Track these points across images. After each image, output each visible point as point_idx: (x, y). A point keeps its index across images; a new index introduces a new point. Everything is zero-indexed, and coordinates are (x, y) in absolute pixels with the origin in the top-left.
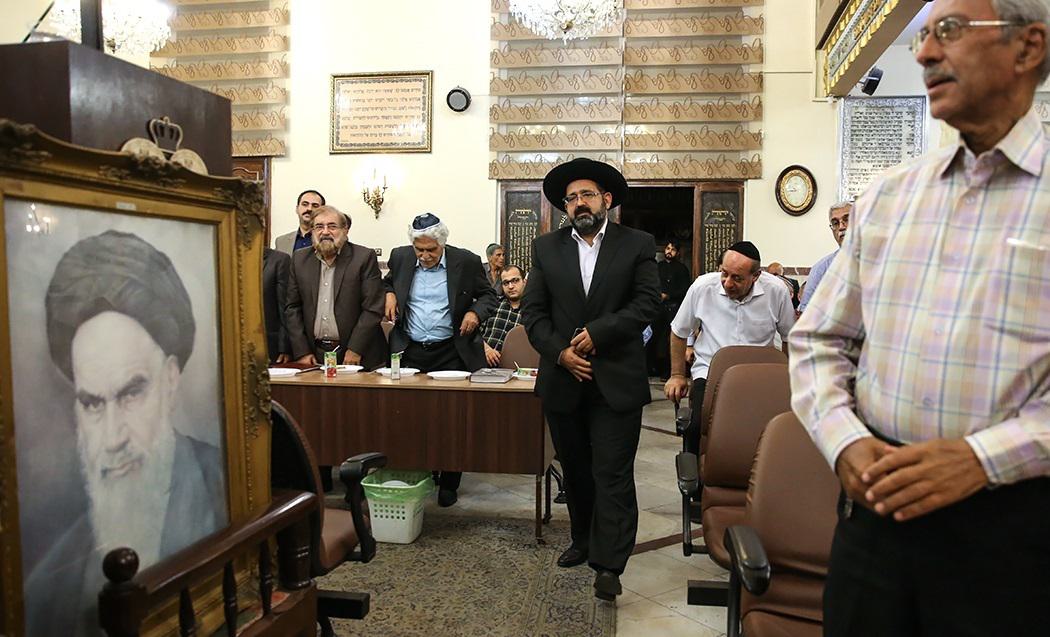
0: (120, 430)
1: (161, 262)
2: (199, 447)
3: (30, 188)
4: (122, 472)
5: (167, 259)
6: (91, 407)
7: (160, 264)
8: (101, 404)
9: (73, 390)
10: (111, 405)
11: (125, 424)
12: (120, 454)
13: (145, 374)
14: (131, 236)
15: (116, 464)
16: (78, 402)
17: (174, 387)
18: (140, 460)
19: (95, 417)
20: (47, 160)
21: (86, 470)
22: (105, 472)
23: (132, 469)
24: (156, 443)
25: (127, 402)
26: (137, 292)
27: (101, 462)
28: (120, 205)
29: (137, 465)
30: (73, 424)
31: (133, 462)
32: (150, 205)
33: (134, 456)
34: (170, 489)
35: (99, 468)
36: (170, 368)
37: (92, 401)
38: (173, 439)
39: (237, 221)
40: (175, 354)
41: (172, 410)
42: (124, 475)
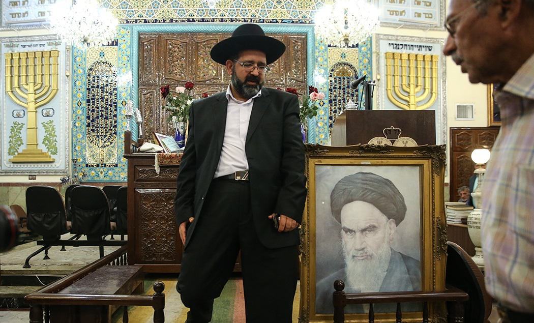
1: (388, 183)
2: (405, 258)
3: (324, 161)
4: (362, 258)
5: (390, 182)
6: (349, 233)
7: (386, 184)
9: (341, 226)
10: (358, 234)
12: (361, 252)
13: (375, 224)
15: (359, 255)
16: (342, 230)
18: (371, 256)
19: (349, 237)
20: (327, 152)
22: (354, 257)
24: (380, 251)
25: (366, 234)
26: (373, 194)
29: (369, 257)
30: (340, 237)
32: (379, 161)
33: (368, 254)
34: (387, 271)
35: (351, 254)
36: (390, 223)
37: (348, 231)
38: (391, 252)
39: (432, 163)
42: (362, 260)
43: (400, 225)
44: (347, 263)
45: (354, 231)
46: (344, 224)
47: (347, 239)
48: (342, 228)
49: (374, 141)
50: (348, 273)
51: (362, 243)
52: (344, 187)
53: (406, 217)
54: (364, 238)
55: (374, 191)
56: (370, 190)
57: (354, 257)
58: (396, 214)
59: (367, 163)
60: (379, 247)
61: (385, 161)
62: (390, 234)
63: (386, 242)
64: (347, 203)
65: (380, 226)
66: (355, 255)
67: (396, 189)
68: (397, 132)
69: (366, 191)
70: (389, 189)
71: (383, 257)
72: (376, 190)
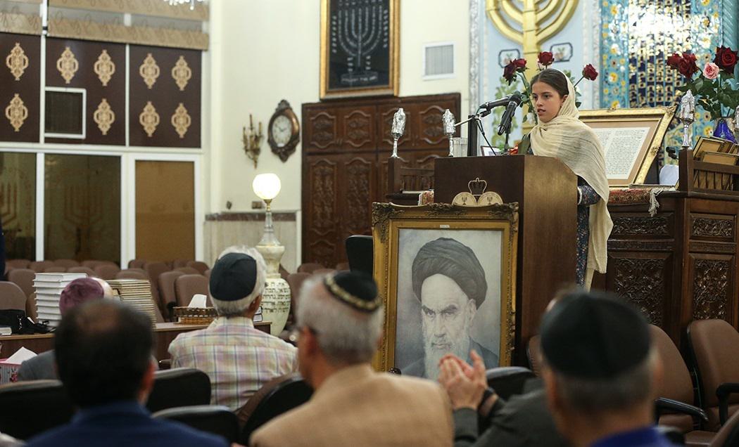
0: (441, 328)
1: (468, 252)
6: (429, 314)
7: (468, 254)
8: (433, 314)
10: (438, 316)
11: (444, 326)
12: (441, 339)
13: (456, 305)
14: (451, 239)
15: (437, 343)
17: (473, 316)
18: (449, 345)
21: (425, 340)
22: (433, 344)
23: (445, 348)
24: (459, 340)
25: (446, 316)
26: (453, 266)
27: (432, 339)
28: (441, 226)
29: (447, 346)
30: (421, 320)
31: (446, 344)
32: (457, 224)
33: (446, 342)
35: (430, 342)
36: (470, 305)
37: (429, 311)
38: (469, 342)
40: (474, 298)
41: (470, 326)
42: (441, 349)
43: (480, 307)
44: (427, 351)
45: (434, 312)
46: (424, 303)
47: (427, 319)
48: (422, 308)
49: (459, 200)
50: (426, 364)
51: (441, 328)
52: (425, 256)
53: (487, 297)
54: (444, 321)
55: (454, 263)
56: (451, 261)
57: (433, 344)
58: (477, 295)
59: (445, 226)
60: (458, 335)
61: (463, 224)
62: (470, 319)
63: (465, 329)
64: (428, 277)
65: (460, 307)
66: (434, 342)
67: (477, 259)
68: (482, 186)
69: (446, 263)
70: (470, 260)
71: (462, 348)
72: (457, 261)
